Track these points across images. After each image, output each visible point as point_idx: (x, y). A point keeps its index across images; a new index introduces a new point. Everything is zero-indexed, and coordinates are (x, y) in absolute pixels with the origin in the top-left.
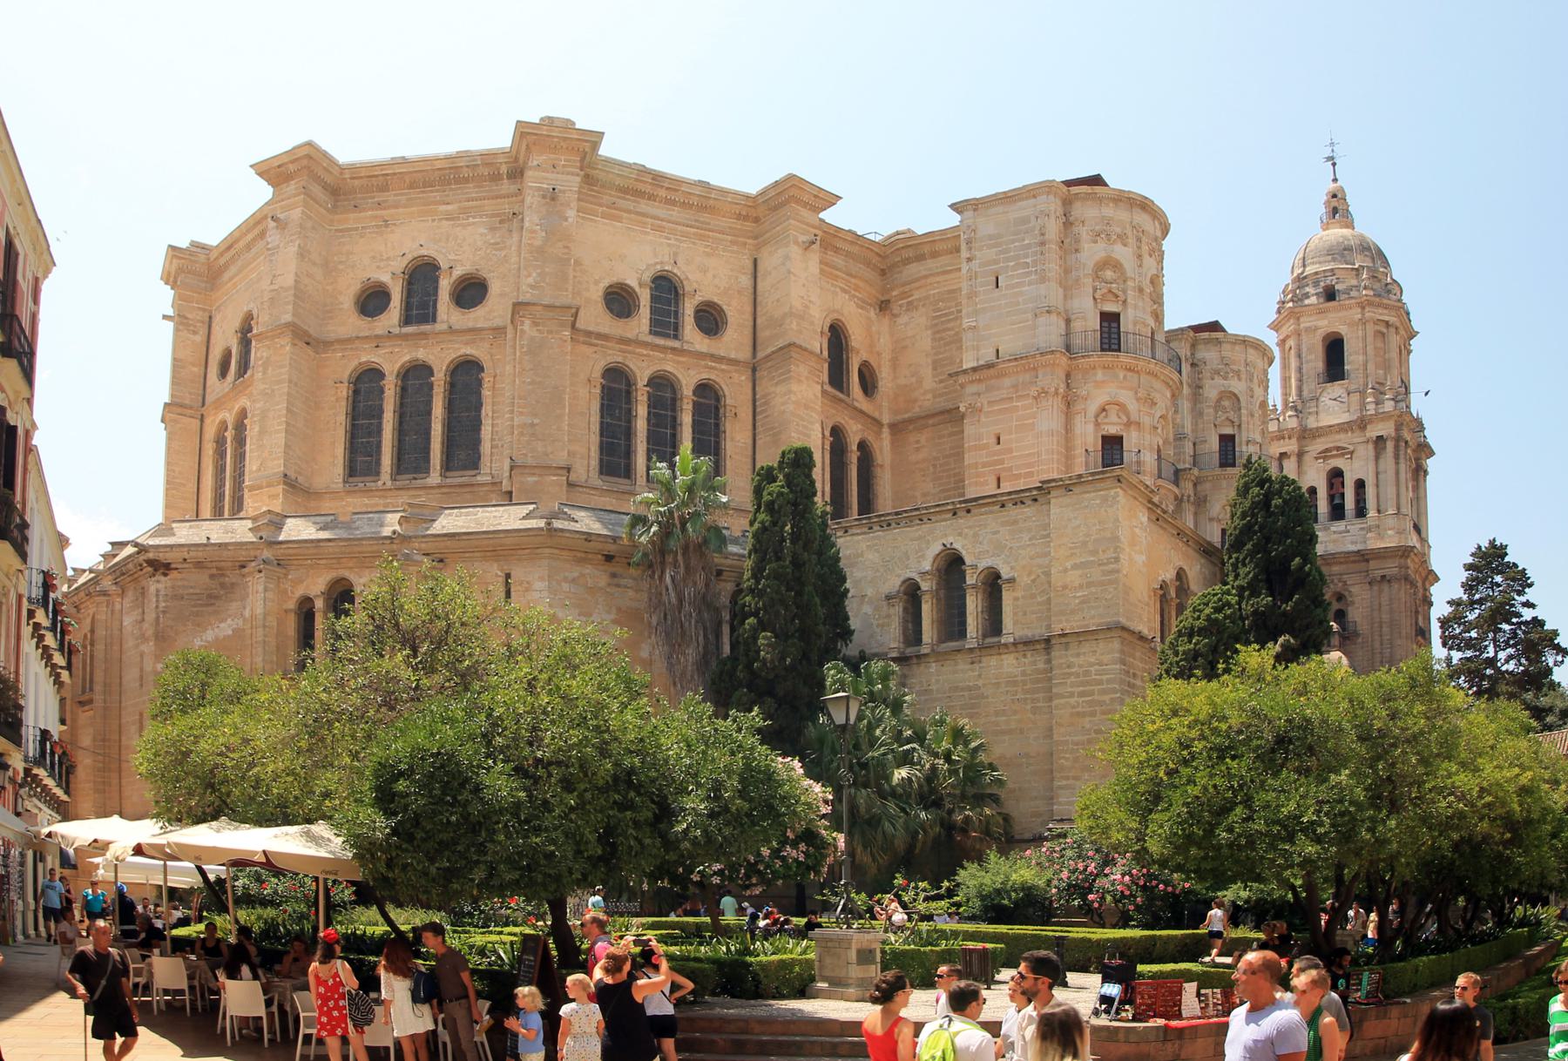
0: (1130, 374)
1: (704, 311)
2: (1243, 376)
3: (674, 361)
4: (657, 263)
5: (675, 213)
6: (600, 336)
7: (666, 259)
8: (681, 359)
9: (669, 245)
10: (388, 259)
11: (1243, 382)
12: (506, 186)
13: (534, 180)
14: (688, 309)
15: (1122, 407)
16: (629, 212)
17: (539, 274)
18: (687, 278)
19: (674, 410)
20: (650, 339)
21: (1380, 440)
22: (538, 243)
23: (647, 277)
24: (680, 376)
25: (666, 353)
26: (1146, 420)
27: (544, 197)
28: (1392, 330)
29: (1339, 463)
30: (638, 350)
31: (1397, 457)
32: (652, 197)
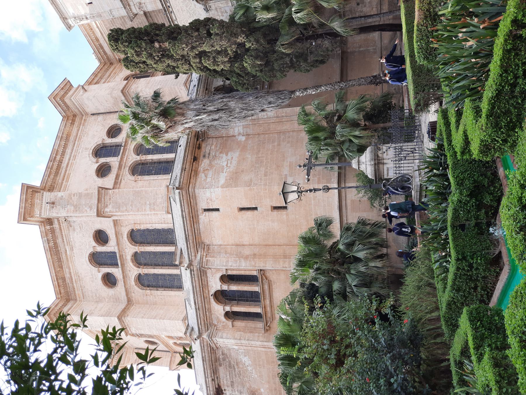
1: (112, 135)
3: (130, 145)
4: (89, 156)
5: (68, 151)
7: (88, 153)
9: (82, 152)
10: (92, 275)
12: (56, 225)
13: (46, 214)
14: (110, 141)
16: (66, 171)
17: (86, 206)
18: (96, 143)
22: (72, 208)
23: (95, 160)
27: (53, 207)
32: (61, 162)
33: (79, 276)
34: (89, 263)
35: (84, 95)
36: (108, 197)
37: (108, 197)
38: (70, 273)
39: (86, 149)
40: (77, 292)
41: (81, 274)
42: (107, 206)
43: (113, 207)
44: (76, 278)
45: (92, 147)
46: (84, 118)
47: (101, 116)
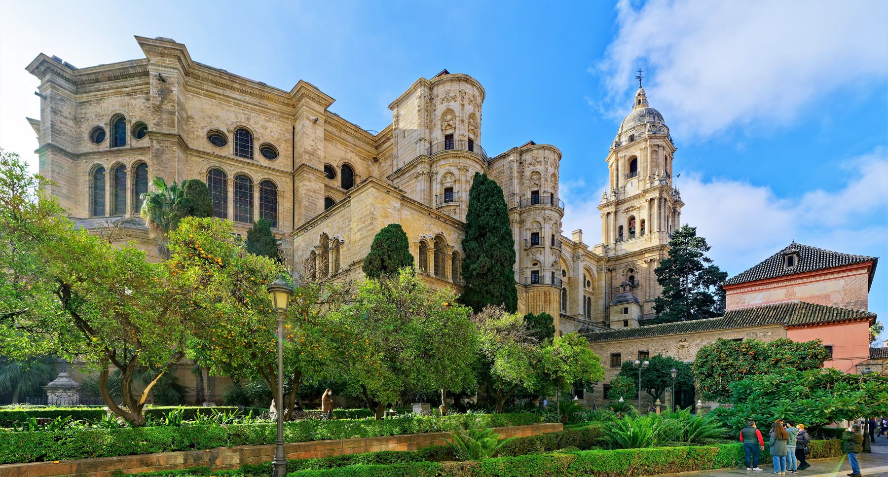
0: (455, 159)
2: (543, 163)
3: (248, 169)
4: (237, 122)
6: (204, 153)
7: (243, 120)
8: (253, 168)
11: (543, 166)
14: (257, 146)
15: (451, 173)
18: (255, 131)
19: (251, 191)
20: (234, 157)
21: (652, 200)
23: (232, 128)
24: (252, 176)
25: (244, 165)
26: (463, 179)
28: (661, 148)
29: (631, 214)
30: (228, 162)
31: (660, 207)
33: (101, 100)
34: (114, 113)
35: (308, 122)
36: (169, 145)
37: (169, 145)
38: (104, 90)
39: (248, 119)
40: (85, 95)
41: (104, 102)
42: (159, 143)
43: (158, 149)
44: (99, 96)
45: (250, 125)
46: (291, 117)
47: (291, 138)
